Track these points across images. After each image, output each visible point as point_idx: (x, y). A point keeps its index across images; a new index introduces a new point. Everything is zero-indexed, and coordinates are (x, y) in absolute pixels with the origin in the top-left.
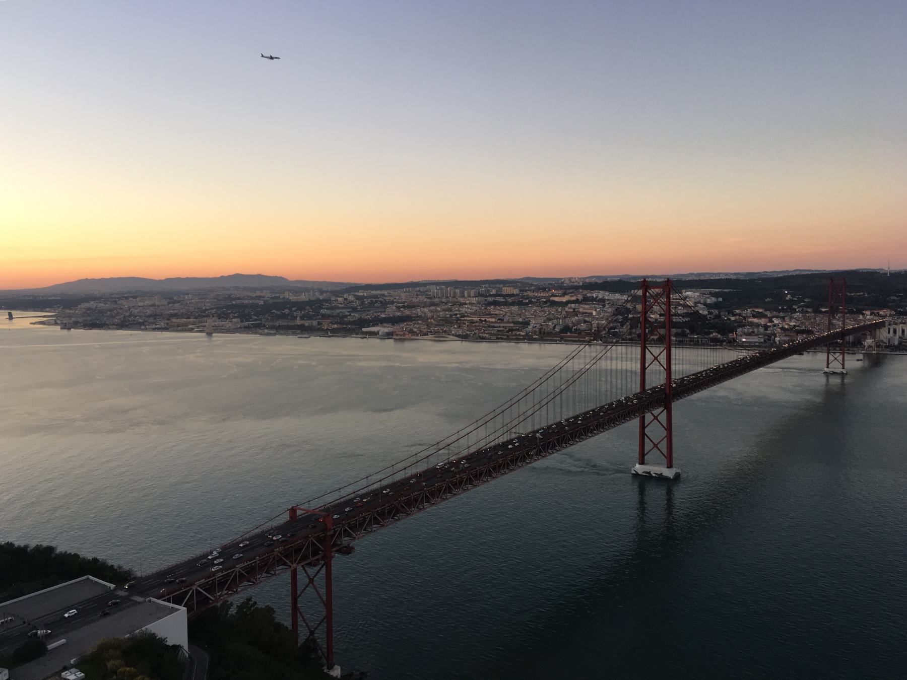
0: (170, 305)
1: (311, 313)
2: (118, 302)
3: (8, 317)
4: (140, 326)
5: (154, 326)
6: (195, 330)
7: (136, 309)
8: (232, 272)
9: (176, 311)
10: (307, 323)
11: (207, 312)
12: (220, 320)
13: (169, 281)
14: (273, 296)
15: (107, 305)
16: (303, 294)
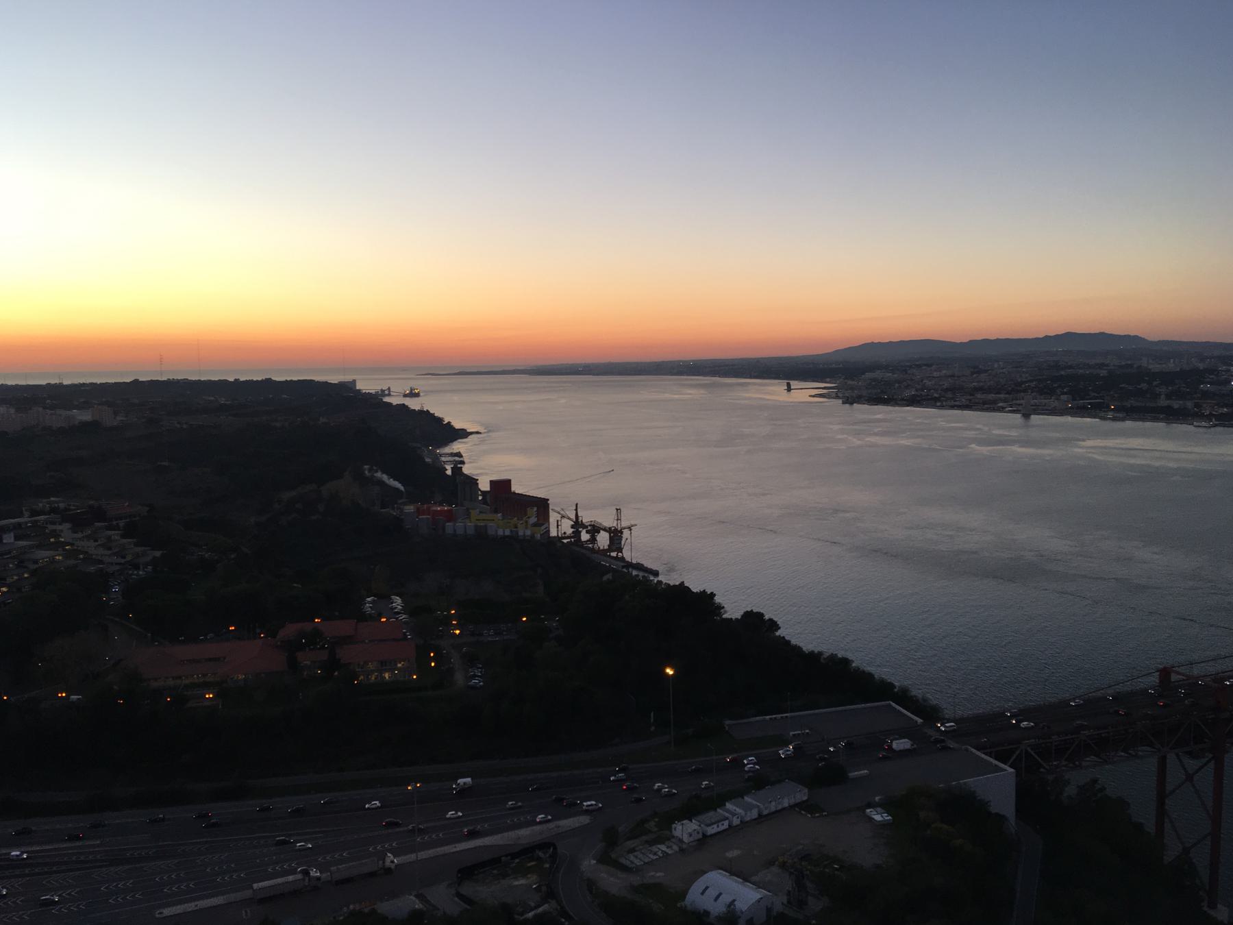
0: (975, 375)
1: (1184, 389)
2: (909, 372)
3: (786, 388)
4: (936, 402)
5: (953, 403)
6: (1007, 409)
7: (930, 381)
8: (1061, 331)
9: (982, 384)
10: (1176, 404)
11: (1023, 386)
12: (1042, 397)
13: (972, 343)
14: (1123, 363)
15: (896, 376)
16: (1172, 361)
